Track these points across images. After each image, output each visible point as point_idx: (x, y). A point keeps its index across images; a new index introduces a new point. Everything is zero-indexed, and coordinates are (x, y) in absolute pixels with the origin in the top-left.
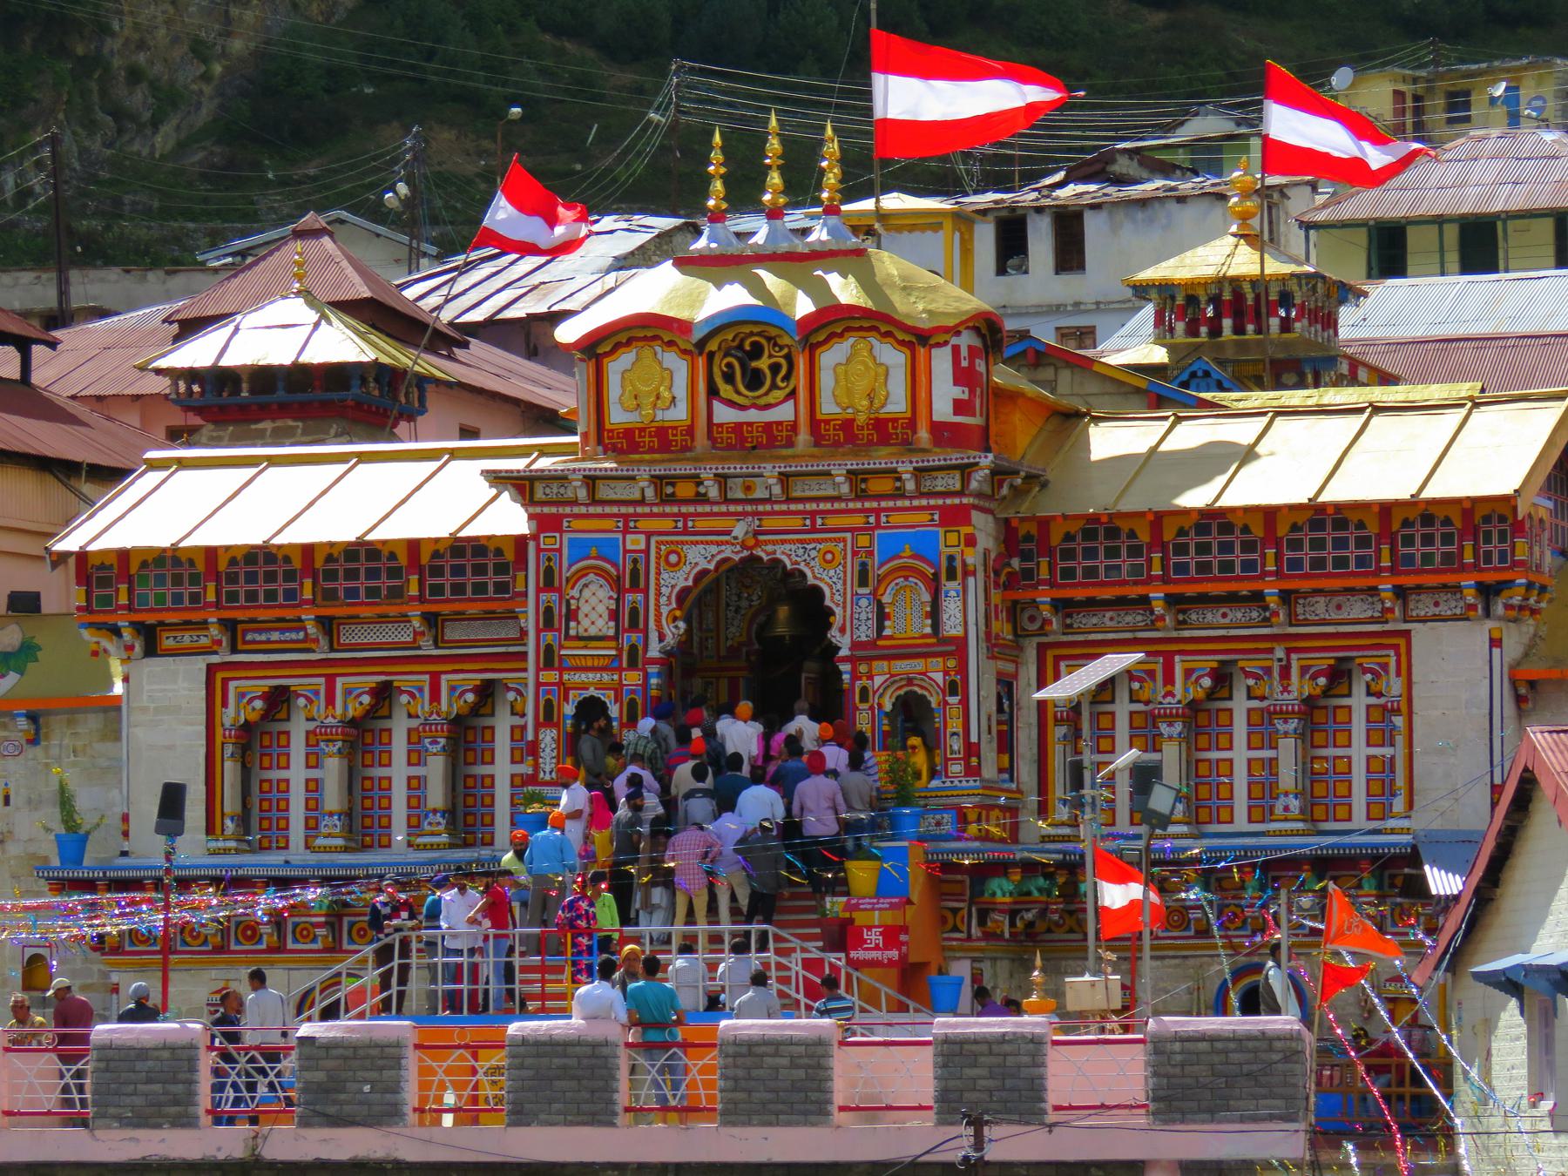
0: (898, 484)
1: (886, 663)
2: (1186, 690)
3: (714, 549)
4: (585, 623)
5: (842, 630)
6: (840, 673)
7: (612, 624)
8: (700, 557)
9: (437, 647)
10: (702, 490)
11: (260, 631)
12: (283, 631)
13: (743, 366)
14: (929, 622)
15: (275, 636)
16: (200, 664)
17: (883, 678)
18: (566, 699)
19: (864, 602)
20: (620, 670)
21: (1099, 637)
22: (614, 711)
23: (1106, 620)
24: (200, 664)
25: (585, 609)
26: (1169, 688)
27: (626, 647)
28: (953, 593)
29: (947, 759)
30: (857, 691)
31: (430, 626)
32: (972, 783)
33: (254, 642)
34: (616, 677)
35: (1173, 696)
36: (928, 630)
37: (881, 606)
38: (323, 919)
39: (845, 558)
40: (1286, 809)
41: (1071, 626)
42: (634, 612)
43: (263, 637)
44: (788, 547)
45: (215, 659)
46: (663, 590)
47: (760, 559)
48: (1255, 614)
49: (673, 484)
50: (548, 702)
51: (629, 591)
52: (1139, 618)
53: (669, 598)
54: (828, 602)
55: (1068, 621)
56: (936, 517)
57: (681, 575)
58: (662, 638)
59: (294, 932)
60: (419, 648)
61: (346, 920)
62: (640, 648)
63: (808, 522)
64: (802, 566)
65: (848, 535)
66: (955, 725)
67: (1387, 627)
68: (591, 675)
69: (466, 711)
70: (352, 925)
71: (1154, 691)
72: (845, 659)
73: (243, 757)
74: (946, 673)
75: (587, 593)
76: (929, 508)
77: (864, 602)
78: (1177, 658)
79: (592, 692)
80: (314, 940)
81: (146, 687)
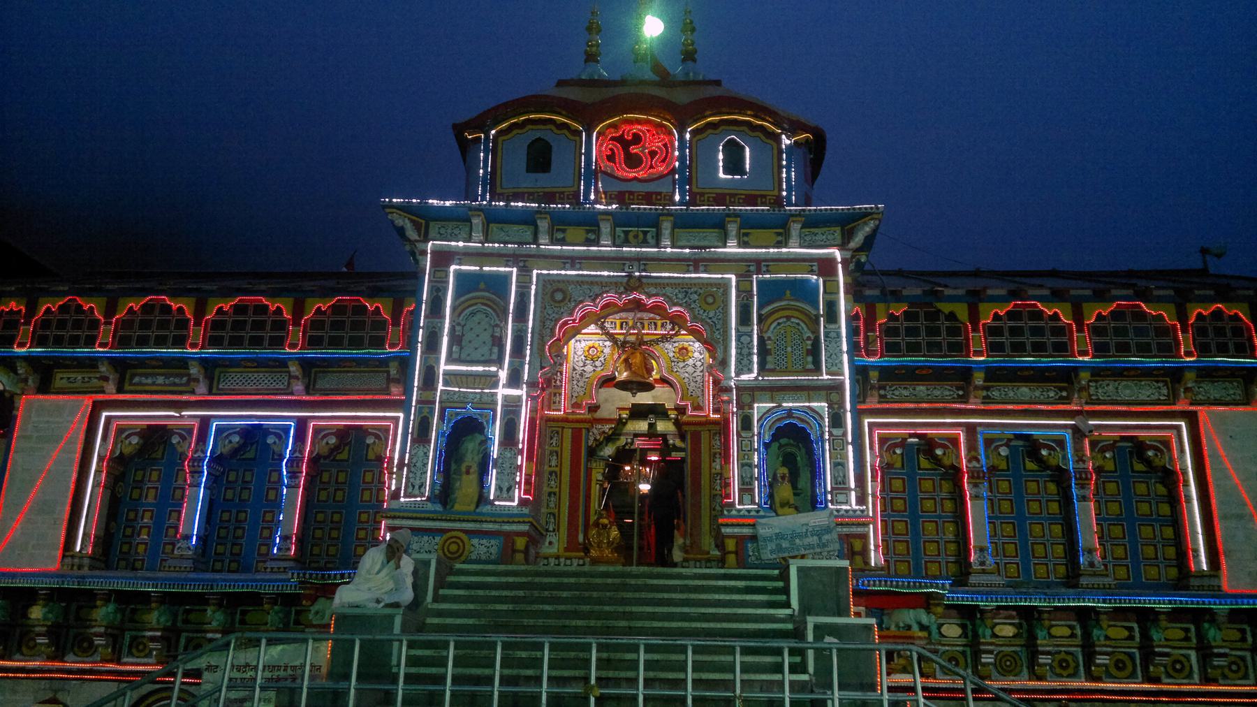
2: (987, 457)
9: (308, 393)
11: (146, 376)
12: (167, 376)
14: (810, 359)
15: (160, 380)
16: (86, 402)
21: (912, 406)
24: (86, 402)
26: (973, 453)
31: (304, 376)
33: (140, 384)
35: (978, 460)
38: (159, 634)
40: (1092, 564)
43: (149, 381)
45: (100, 397)
46: (548, 323)
48: (1052, 394)
49: (564, 231)
55: (882, 392)
59: (130, 646)
60: (292, 394)
61: (184, 635)
67: (1178, 408)
69: (325, 451)
70: (189, 640)
73: (116, 483)
78: (979, 429)
80: (149, 655)
81: (34, 419)
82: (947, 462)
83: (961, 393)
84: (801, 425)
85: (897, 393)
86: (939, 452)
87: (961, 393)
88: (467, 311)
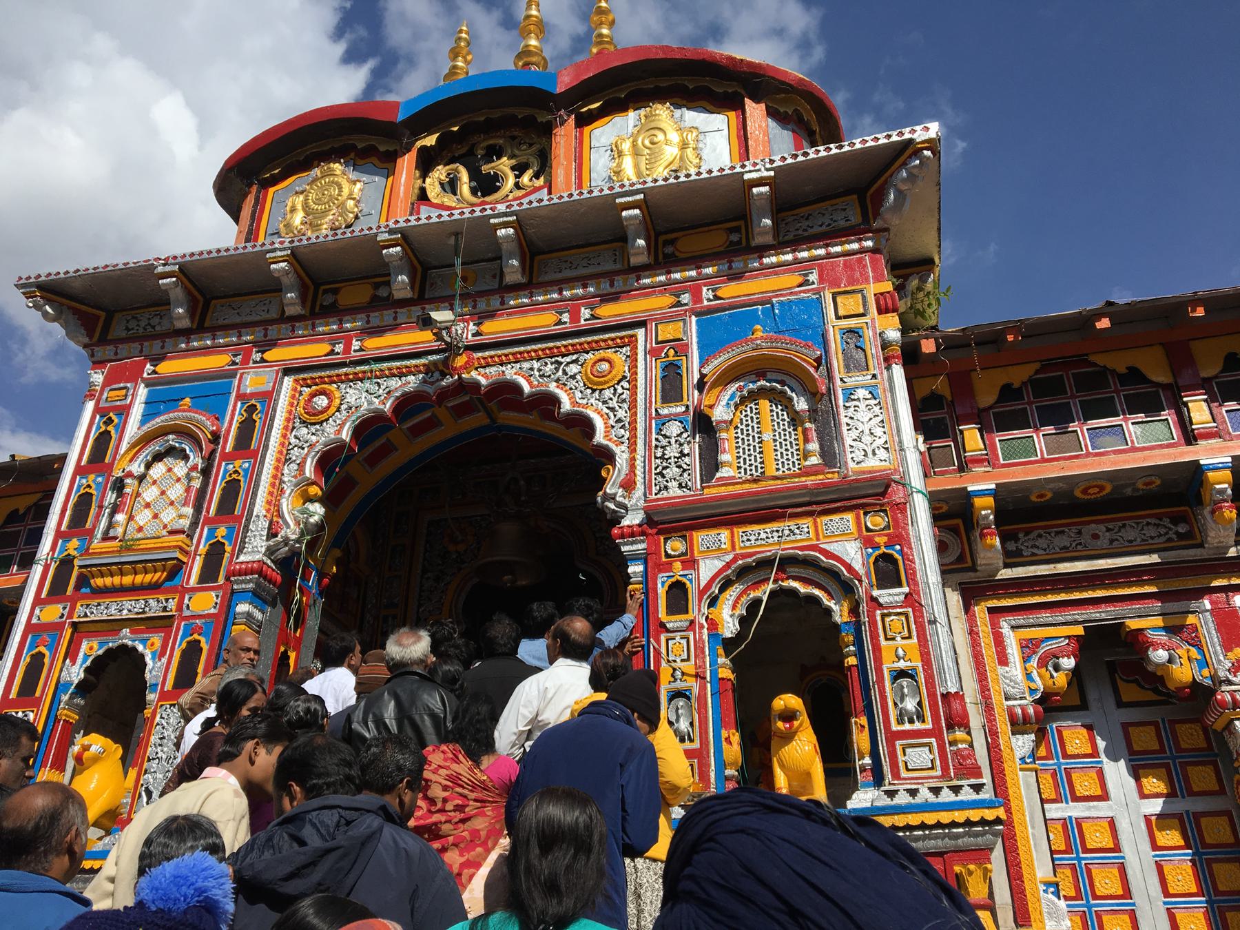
0: (734, 237)
1: (724, 534)
3: (394, 383)
4: (143, 517)
5: (628, 485)
6: (623, 561)
7: (189, 511)
8: (364, 398)
10: (383, 292)
13: (475, 174)
17: (719, 564)
18: (71, 653)
19: (674, 429)
20: (184, 591)
22: (158, 669)
23: (1086, 538)
25: (150, 493)
27: (203, 548)
28: (862, 393)
29: (893, 736)
30: (662, 591)
32: (967, 795)
34: (172, 604)
36: (814, 460)
37: (703, 425)
39: (633, 367)
41: (1018, 553)
42: (232, 489)
44: (526, 365)
47: (477, 385)
50: (37, 660)
51: (227, 458)
52: (1152, 532)
53: (301, 466)
54: (600, 438)
56: (813, 277)
57: (330, 429)
58: (272, 534)
62: (228, 548)
63: (566, 317)
64: (553, 387)
65: (640, 333)
66: (897, 651)
68: (127, 605)
71: (1205, 663)
72: (632, 533)
74: (868, 542)
75: (158, 470)
76: (796, 261)
77: (674, 429)
79: (126, 637)
82: (1183, 672)
83: (1182, 529)
84: (802, 589)
85: (1042, 543)
86: (1160, 655)
87: (1182, 529)
88: (155, 447)
